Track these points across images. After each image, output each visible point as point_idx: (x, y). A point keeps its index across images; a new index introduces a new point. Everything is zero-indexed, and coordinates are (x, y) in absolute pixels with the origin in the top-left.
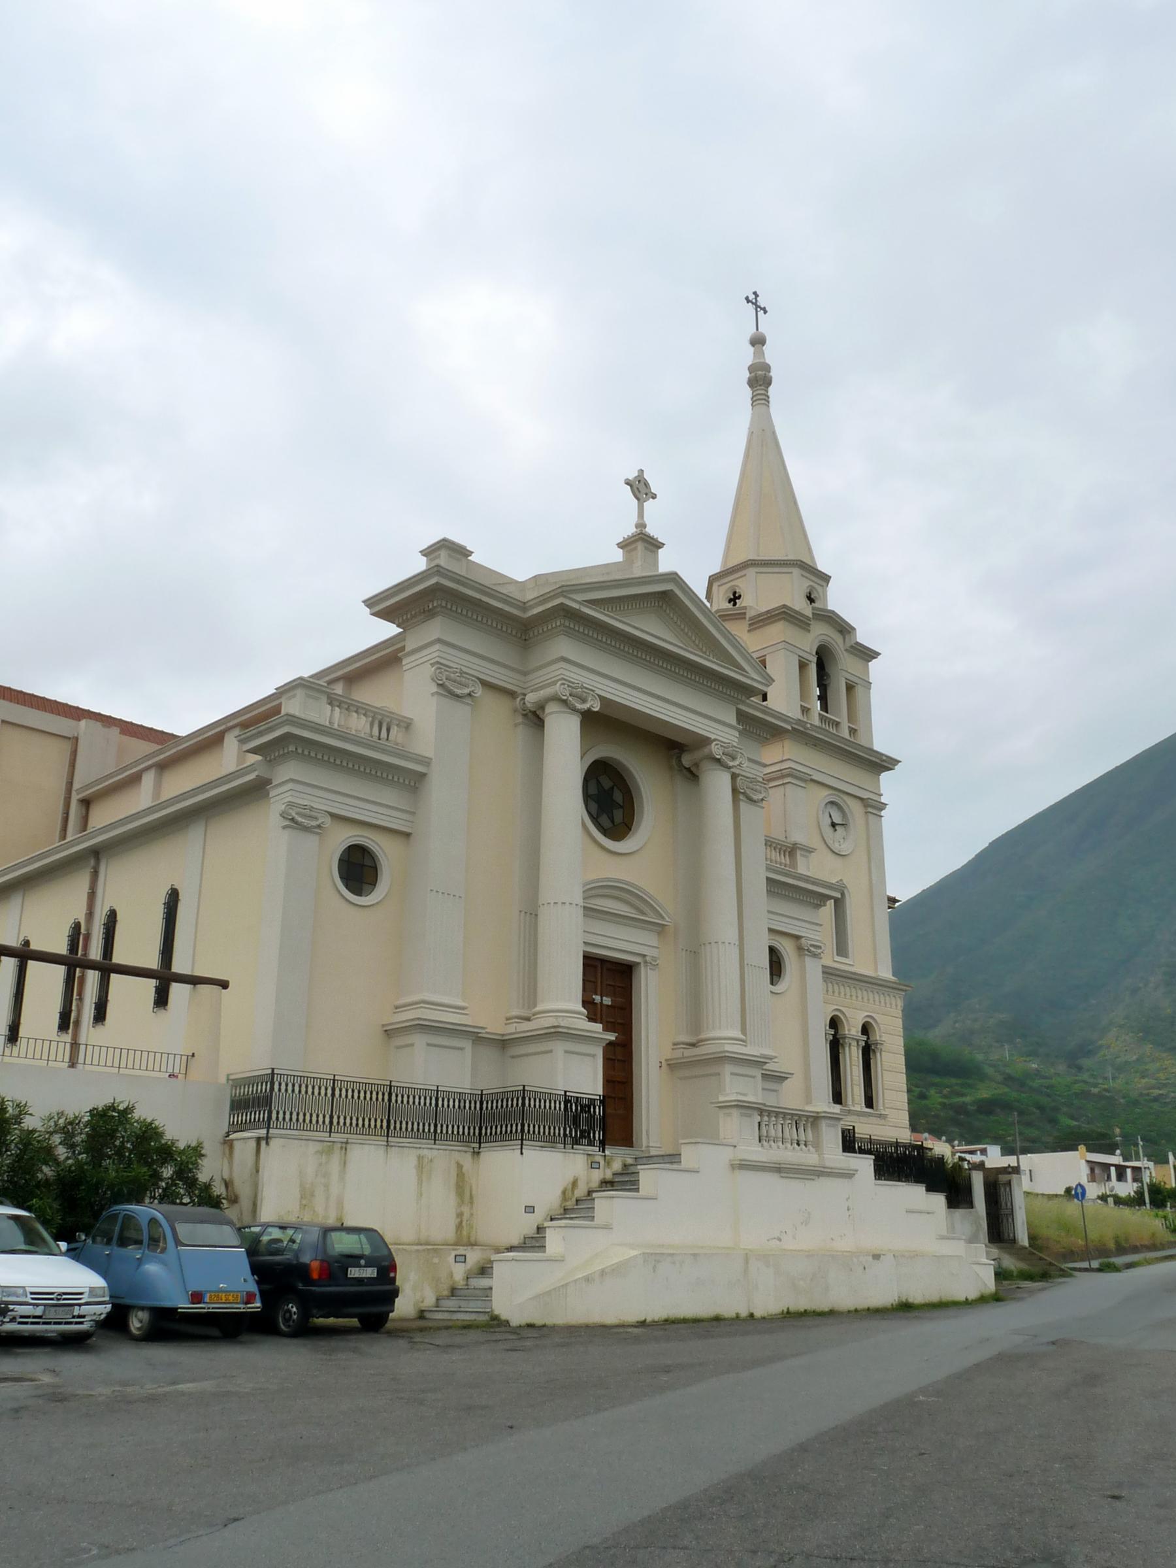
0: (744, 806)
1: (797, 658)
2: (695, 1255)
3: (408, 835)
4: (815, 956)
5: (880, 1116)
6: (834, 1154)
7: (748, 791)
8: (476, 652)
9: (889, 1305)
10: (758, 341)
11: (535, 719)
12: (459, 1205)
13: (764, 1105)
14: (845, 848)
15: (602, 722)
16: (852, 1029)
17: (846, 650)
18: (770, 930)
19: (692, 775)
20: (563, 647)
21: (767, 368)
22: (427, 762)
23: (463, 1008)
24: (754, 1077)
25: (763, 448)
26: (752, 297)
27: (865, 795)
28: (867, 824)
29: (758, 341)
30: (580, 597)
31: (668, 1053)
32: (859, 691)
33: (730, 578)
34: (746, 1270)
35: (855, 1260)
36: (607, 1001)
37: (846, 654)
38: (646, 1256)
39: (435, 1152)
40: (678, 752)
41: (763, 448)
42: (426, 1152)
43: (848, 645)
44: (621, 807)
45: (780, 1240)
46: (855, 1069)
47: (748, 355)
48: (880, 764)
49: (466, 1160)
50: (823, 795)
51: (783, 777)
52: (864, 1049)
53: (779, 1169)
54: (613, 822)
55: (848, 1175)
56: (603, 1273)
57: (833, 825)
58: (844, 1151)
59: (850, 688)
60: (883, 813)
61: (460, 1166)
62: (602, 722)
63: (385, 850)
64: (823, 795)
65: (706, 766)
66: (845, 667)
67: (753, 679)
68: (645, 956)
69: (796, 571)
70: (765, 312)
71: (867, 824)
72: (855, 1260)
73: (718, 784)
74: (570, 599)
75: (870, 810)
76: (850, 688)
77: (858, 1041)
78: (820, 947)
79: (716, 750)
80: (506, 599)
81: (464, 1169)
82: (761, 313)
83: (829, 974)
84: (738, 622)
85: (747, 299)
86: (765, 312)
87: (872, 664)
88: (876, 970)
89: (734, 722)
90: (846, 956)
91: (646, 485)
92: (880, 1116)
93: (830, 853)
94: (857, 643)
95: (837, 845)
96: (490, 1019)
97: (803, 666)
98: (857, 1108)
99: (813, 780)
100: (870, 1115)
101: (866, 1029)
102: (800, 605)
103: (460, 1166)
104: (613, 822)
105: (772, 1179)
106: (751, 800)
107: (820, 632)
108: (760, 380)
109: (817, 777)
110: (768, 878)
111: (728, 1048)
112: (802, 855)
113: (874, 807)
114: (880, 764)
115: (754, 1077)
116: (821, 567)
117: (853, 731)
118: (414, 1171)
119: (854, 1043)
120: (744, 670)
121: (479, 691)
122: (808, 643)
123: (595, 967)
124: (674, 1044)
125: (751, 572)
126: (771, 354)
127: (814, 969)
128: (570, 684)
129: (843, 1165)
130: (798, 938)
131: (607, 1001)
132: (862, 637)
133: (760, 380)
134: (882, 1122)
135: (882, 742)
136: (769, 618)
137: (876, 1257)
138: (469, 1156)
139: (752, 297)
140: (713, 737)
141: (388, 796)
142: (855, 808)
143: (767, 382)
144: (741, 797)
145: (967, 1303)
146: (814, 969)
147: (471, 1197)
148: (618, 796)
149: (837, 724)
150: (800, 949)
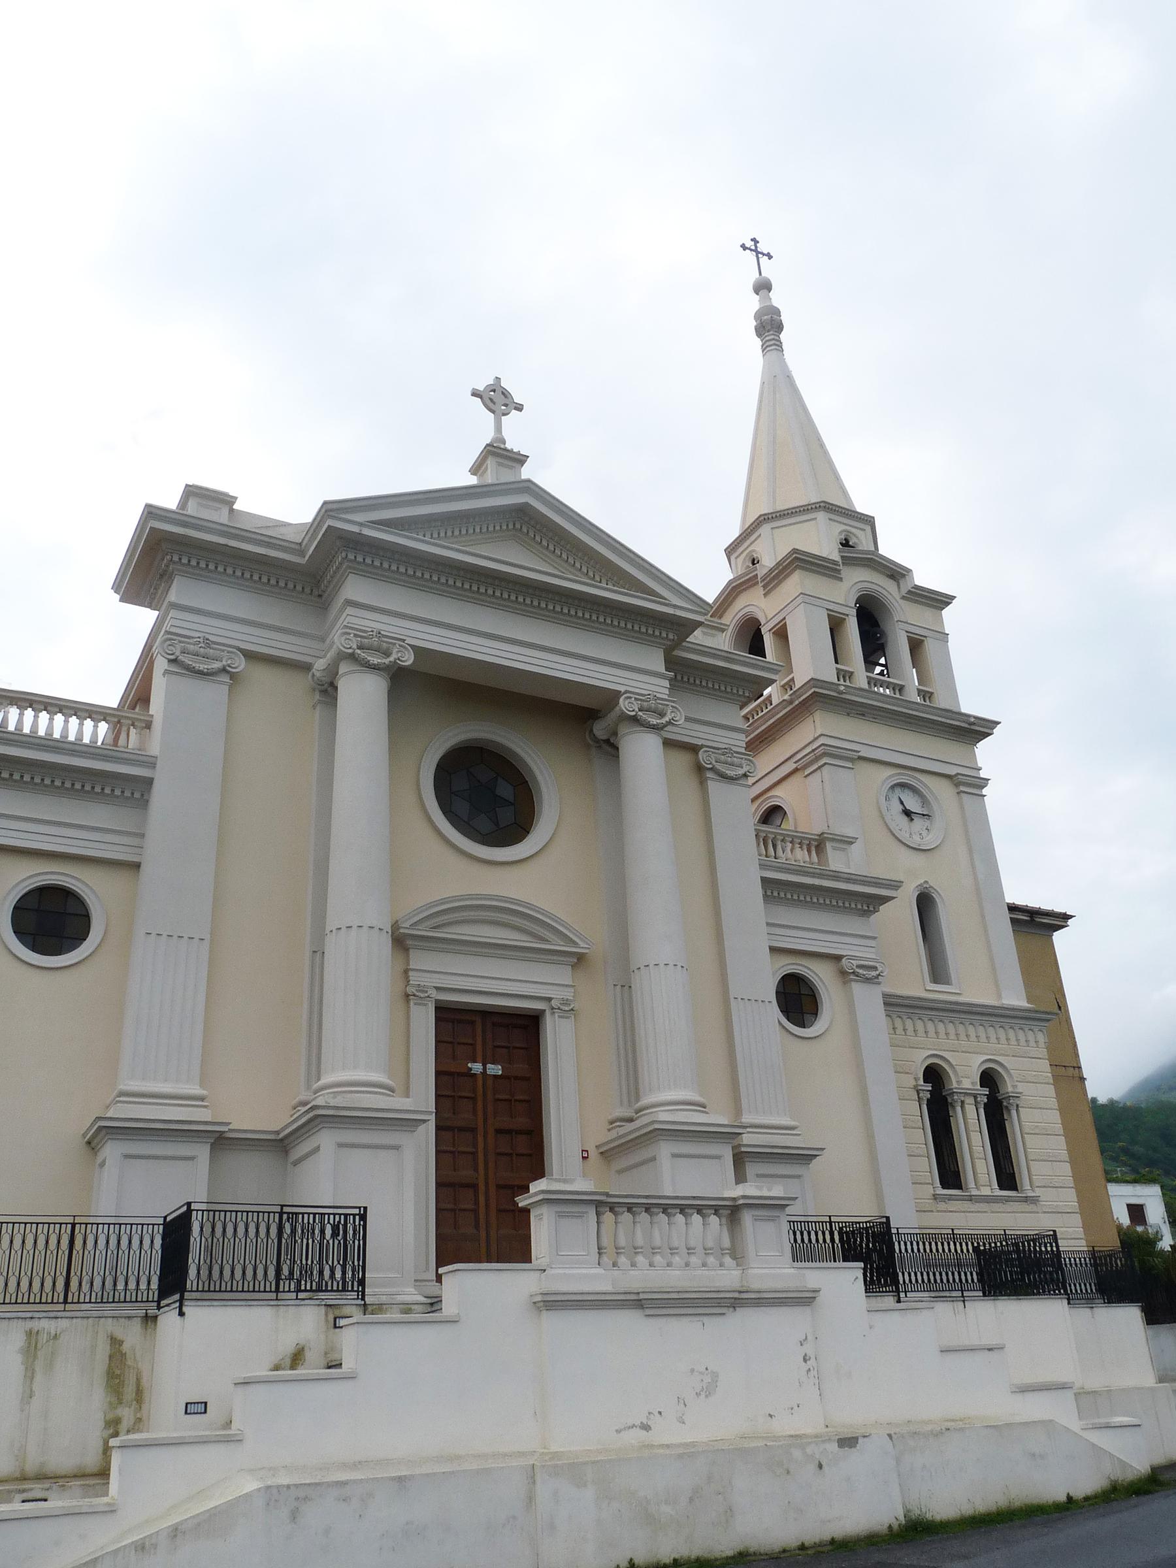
0: (715, 787)
1: (825, 613)
2: (400, 1479)
3: (137, 866)
4: (868, 980)
5: (1026, 1199)
6: (769, 1261)
7: (718, 766)
8: (229, 615)
9: (883, 1529)
10: (763, 287)
11: (328, 691)
12: (112, 1407)
13: (607, 1195)
14: (930, 841)
15: (424, 685)
16: (964, 1078)
17: (903, 598)
18: (773, 949)
19: (610, 748)
20: (354, 588)
21: (777, 312)
22: (151, 764)
23: (202, 1099)
24: (718, 1157)
25: (781, 399)
26: (750, 244)
27: (952, 770)
28: (962, 807)
29: (763, 287)
30: (360, 517)
31: (599, 1135)
32: (930, 646)
33: (746, 545)
34: (530, 1499)
35: (797, 1454)
36: (495, 1069)
37: (902, 602)
38: (272, 1495)
39: (63, 1324)
40: (585, 721)
41: (781, 399)
42: (45, 1324)
43: (904, 591)
44: (512, 804)
45: (646, 1427)
46: (976, 1138)
47: (754, 303)
48: (974, 730)
49: (132, 1335)
50: (883, 777)
51: (817, 759)
52: (987, 1107)
53: (638, 1302)
54: (497, 824)
55: (805, 1299)
56: (175, 1532)
57: (908, 813)
58: (795, 1258)
59: (916, 645)
60: (984, 791)
61: (115, 1342)
62: (424, 685)
63: (91, 886)
64: (883, 777)
65: (623, 729)
66: (904, 619)
67: (675, 606)
68: (549, 999)
69: (821, 516)
70: (770, 257)
71: (962, 807)
72: (797, 1454)
73: (643, 754)
74: (340, 519)
75: (962, 788)
76: (916, 645)
77: (975, 1097)
78: (875, 968)
79: (626, 706)
80: (269, 542)
81: (126, 1347)
82: (764, 259)
83: (893, 1004)
84: (752, 590)
85: (744, 247)
86: (770, 257)
87: (946, 613)
88: (999, 996)
89: (661, 668)
90: (947, 982)
91: (505, 394)
92: (1026, 1199)
93: (903, 848)
94: (917, 587)
95: (917, 838)
96: (254, 1110)
97: (836, 626)
98: (986, 1191)
99: (861, 758)
100: (1008, 1200)
101: (989, 1078)
102: (829, 549)
103: (115, 1342)
104: (497, 824)
105: (629, 1319)
106: (724, 777)
107: (855, 582)
108: (769, 326)
109: (866, 752)
110: (765, 881)
111: (663, 1117)
112: (834, 849)
113: (971, 785)
114: (974, 730)
115: (718, 1157)
116: (861, 507)
117: (926, 695)
118: (19, 1358)
119: (970, 1100)
120: (652, 593)
121: (240, 664)
122: (843, 594)
123: (473, 1023)
124: (611, 1123)
125: (765, 529)
126: (777, 298)
127: (869, 1000)
128: (359, 633)
129: (792, 1284)
130: (838, 958)
131: (495, 1069)
132: (923, 578)
133: (769, 326)
134: (1031, 1207)
135: (971, 704)
136: (781, 572)
137: (848, 1442)
138: (136, 1326)
139: (750, 244)
140: (622, 689)
141: (98, 814)
142: (942, 792)
143: (779, 327)
144: (709, 775)
145: (1070, 1506)
146: (869, 1000)
147: (139, 1392)
148: (505, 790)
149: (901, 689)
150: (844, 975)
